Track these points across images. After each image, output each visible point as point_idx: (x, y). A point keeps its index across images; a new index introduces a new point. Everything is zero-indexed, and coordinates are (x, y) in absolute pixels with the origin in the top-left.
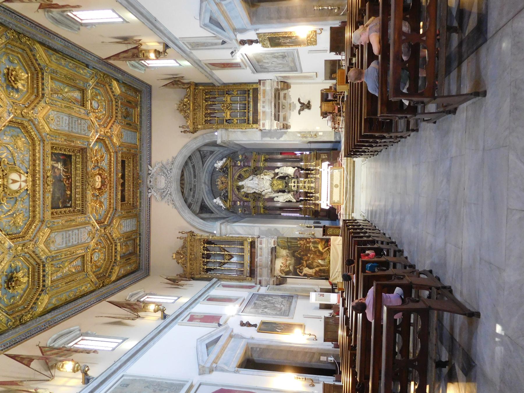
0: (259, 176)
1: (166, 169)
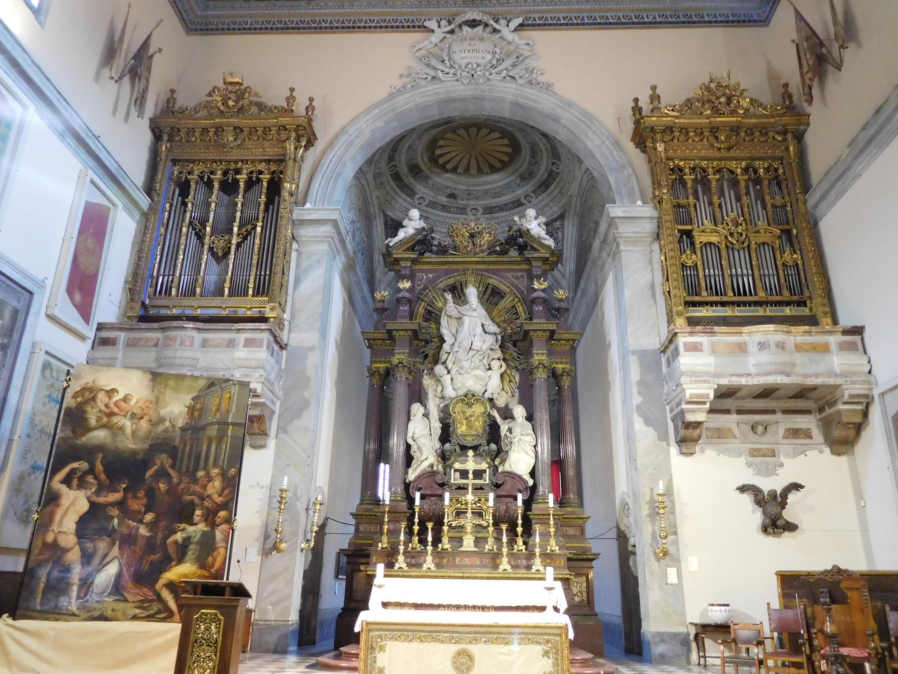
0: (499, 354)
1: (514, 65)
